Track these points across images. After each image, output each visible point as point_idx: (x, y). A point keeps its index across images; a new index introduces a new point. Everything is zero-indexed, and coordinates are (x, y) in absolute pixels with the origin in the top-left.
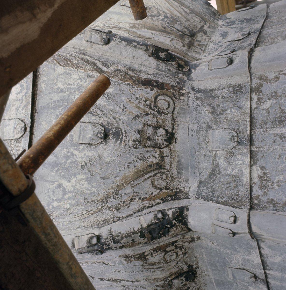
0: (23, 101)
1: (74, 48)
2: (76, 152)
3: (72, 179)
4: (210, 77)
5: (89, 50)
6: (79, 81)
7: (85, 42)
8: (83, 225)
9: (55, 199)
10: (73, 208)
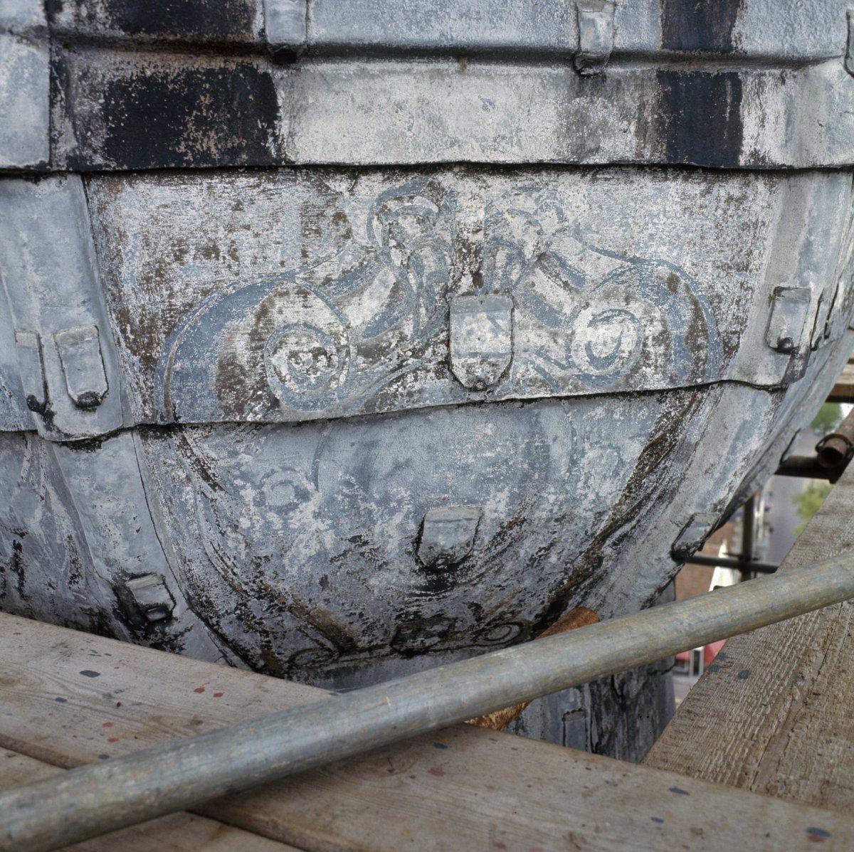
0: (563, 368)
1: (683, 479)
2: (398, 518)
3: (323, 522)
4: (549, 715)
5: (669, 511)
6: (592, 496)
7: (691, 512)
8: (193, 566)
9: (265, 489)
10: (240, 537)
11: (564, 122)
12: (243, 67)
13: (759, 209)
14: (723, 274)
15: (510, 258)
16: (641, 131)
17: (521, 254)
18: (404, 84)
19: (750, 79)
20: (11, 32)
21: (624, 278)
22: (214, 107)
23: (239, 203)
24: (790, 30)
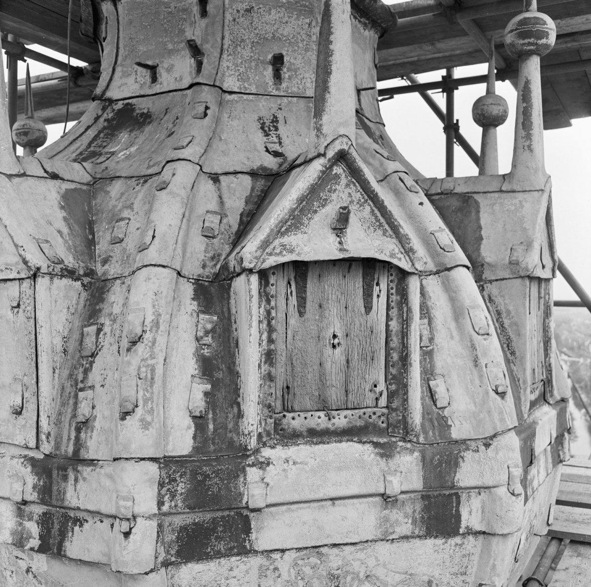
11: (379, 522)
12: (237, 513)
13: (470, 548)
14: (454, 577)
15: (353, 579)
16: (414, 522)
17: (358, 576)
18: (306, 513)
19: (464, 494)
20: (143, 517)
21: (407, 583)
22: (224, 531)
23: (232, 568)
24: (482, 475)
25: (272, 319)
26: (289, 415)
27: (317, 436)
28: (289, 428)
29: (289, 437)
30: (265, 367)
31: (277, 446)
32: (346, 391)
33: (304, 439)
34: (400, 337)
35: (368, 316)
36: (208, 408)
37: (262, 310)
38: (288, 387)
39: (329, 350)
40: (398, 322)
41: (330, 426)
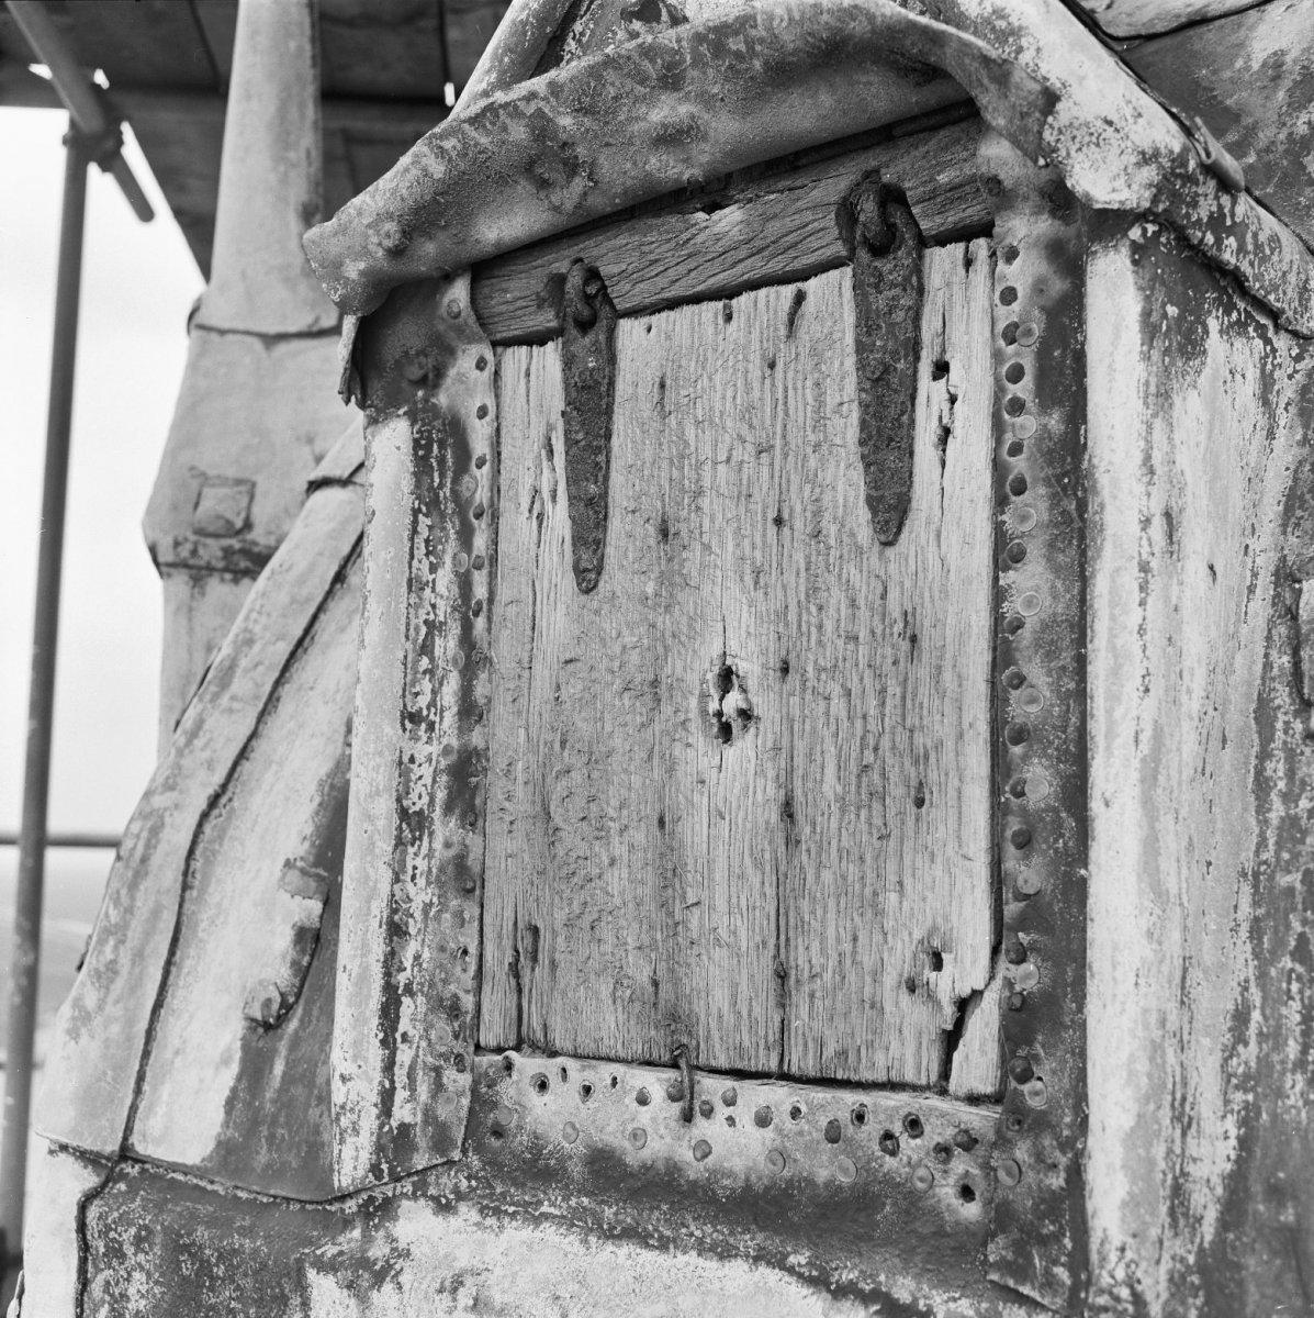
25: (476, 614)
26: (528, 1065)
27: (636, 1197)
28: (520, 1127)
29: (503, 1168)
30: (445, 829)
31: (463, 1207)
32: (782, 976)
33: (566, 1199)
34: (1067, 658)
35: (890, 552)
36: (298, 996)
37: (445, 579)
38: (535, 931)
39: (700, 751)
40: (1057, 570)
41: (685, 1155)
